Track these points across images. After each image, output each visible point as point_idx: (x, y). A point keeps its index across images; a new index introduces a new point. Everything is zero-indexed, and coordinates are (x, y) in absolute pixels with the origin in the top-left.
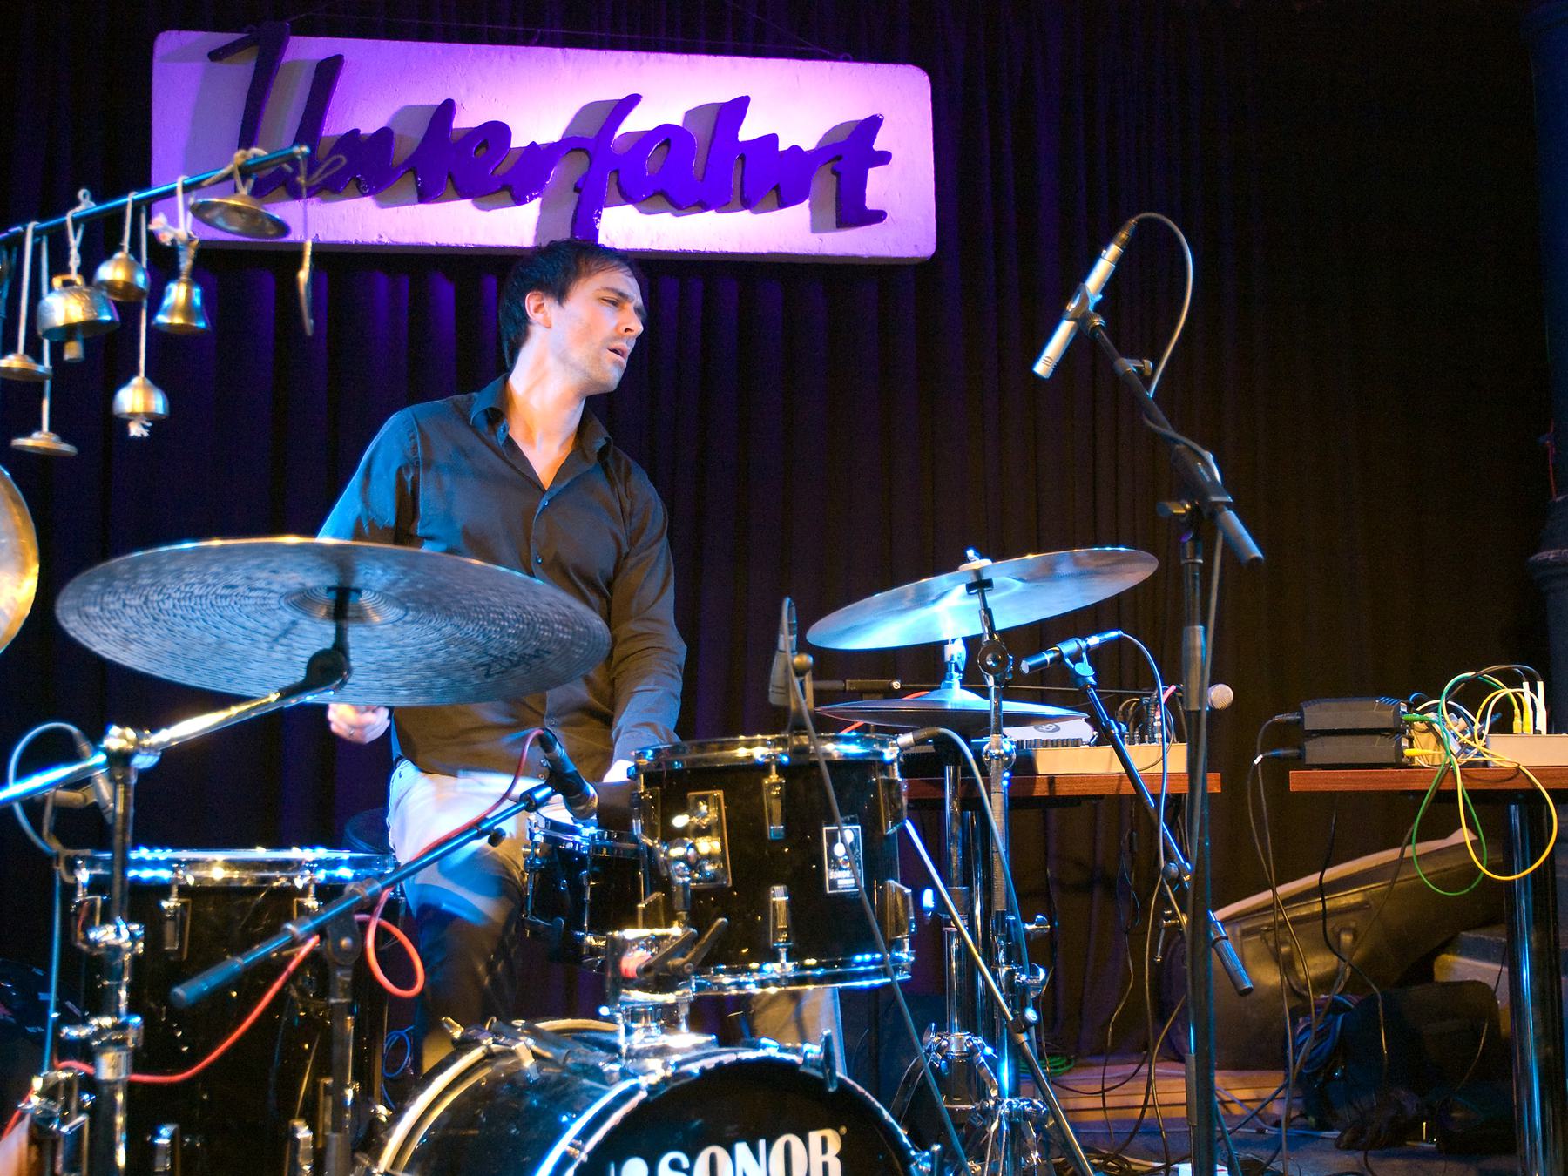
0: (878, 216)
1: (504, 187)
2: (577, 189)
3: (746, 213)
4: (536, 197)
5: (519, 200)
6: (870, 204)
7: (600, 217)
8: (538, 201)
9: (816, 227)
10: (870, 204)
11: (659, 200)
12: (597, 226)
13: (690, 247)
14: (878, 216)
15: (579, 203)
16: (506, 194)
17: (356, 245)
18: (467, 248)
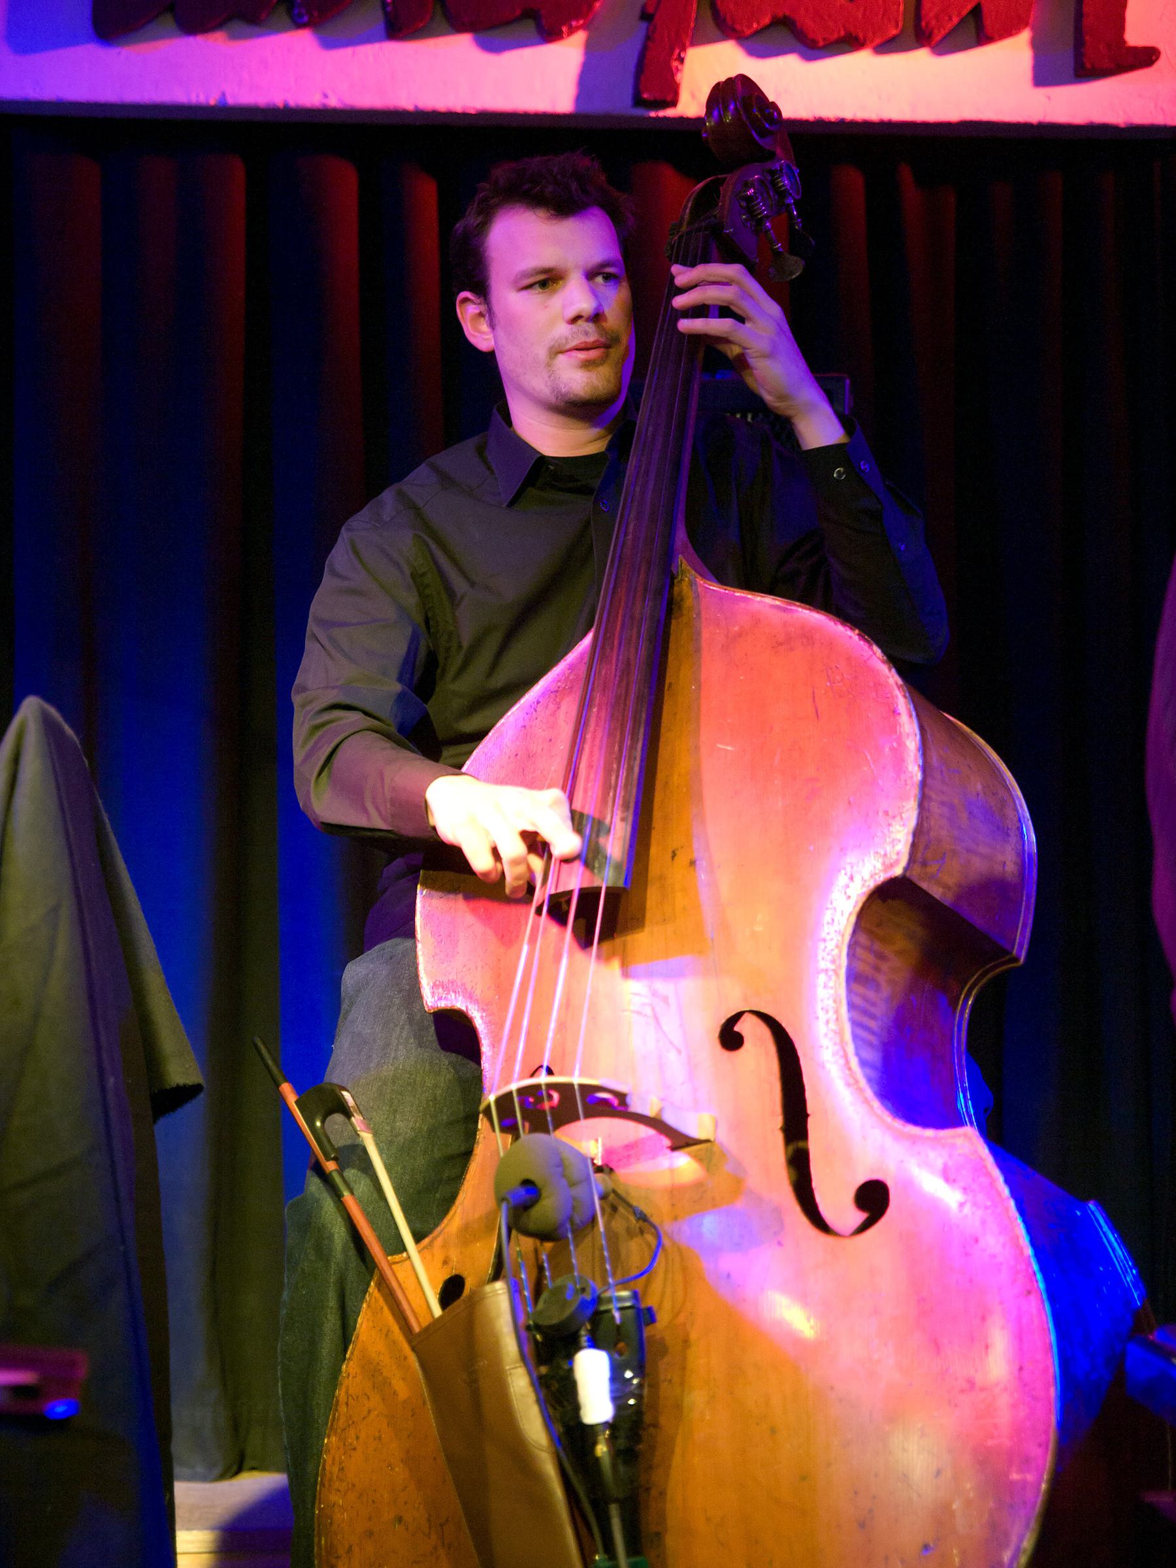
0: (1146, 57)
1: (530, 14)
2: (646, 16)
3: (922, 56)
4: (577, 28)
5: (550, 34)
6: (1134, 36)
7: (682, 60)
8: (579, 37)
9: (1043, 76)
10: (1134, 36)
11: (782, 34)
12: (678, 77)
13: (830, 112)
14: (1146, 57)
15: (648, 37)
16: (529, 26)
17: (288, 111)
18: (465, 115)
